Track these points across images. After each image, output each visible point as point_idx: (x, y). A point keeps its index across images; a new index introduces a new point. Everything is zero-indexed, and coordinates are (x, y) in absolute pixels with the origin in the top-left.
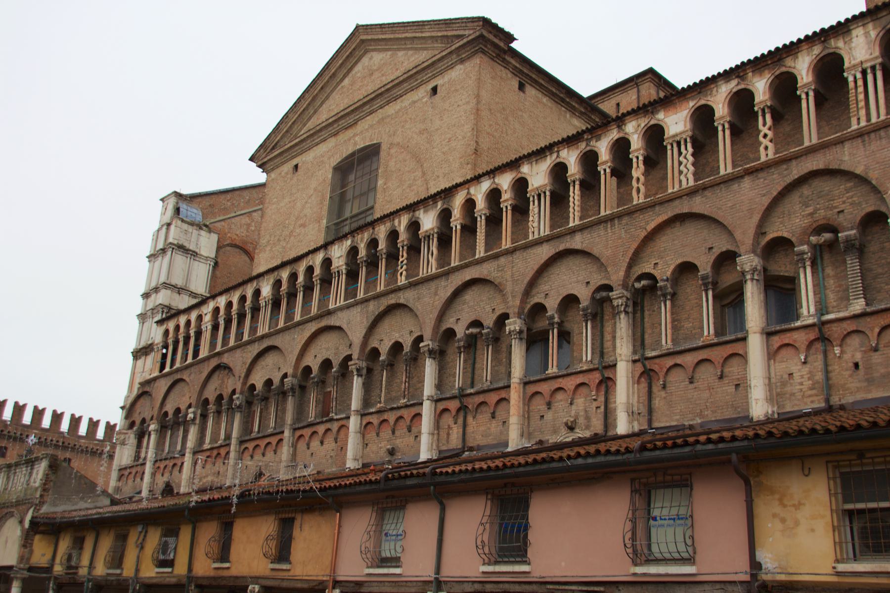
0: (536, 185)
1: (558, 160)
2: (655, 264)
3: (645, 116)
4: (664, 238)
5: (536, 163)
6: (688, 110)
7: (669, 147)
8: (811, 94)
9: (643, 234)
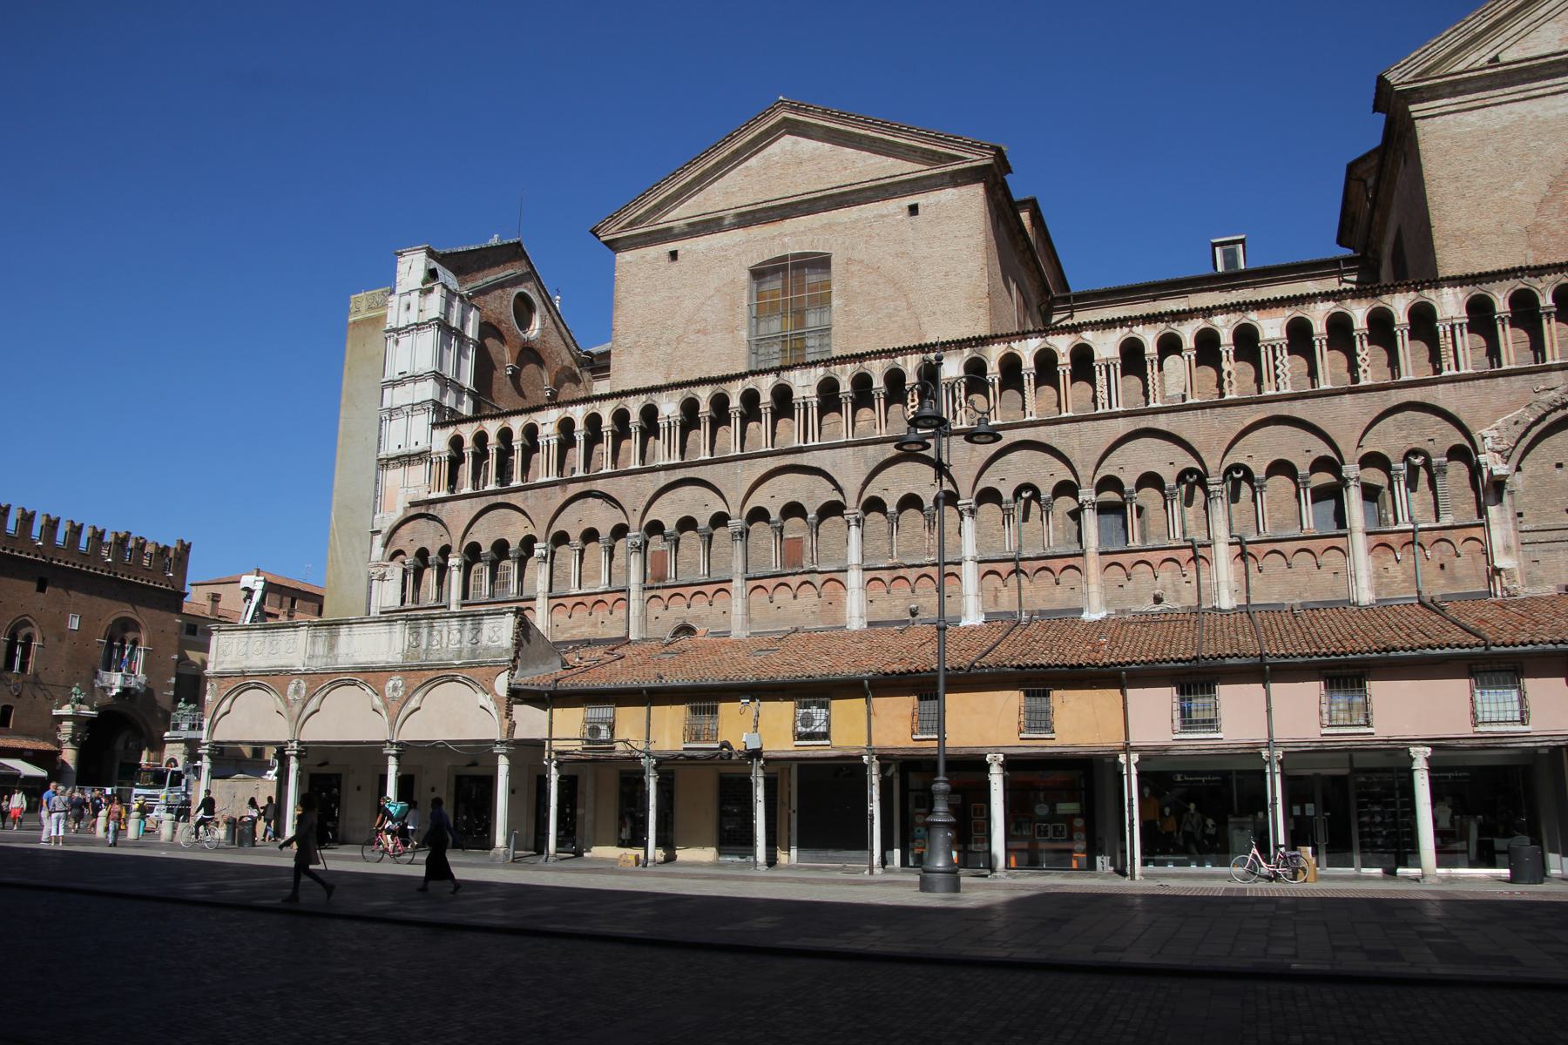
0: (1104, 356)
1: (1131, 335)
6: (1283, 319)
8: (1406, 332)
9: (1240, 428)
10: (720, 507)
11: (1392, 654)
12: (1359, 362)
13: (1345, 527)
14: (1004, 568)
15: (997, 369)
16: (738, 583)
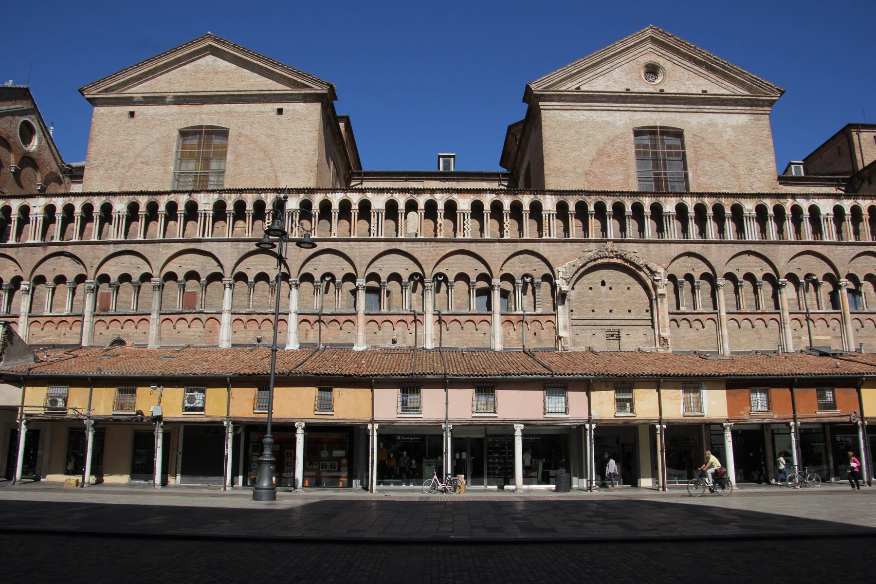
0: (376, 208)
1: (392, 198)
8: (528, 215)
9: (444, 254)
10: (147, 269)
11: (509, 376)
12: (505, 227)
13: (491, 310)
14: (312, 319)
15: (318, 207)
16: (154, 316)
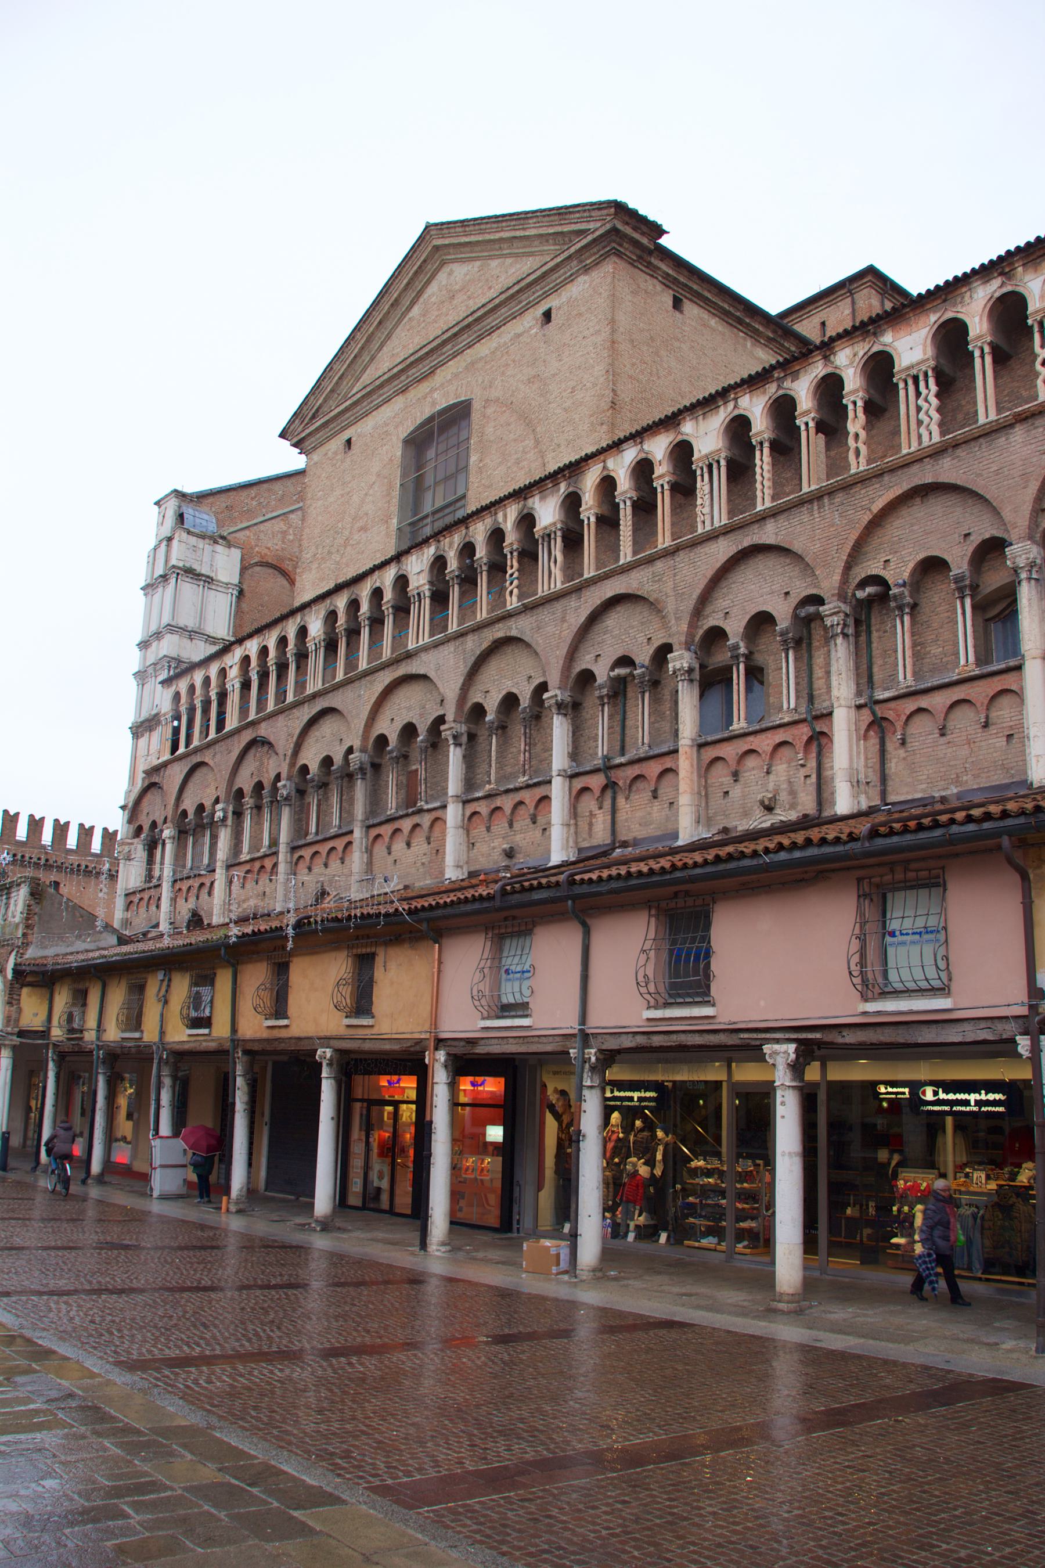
1: (736, 412)
2: (886, 561)
3: (864, 340)
4: (897, 523)
5: (704, 419)
6: (928, 328)
7: (901, 385)
9: (867, 517)
